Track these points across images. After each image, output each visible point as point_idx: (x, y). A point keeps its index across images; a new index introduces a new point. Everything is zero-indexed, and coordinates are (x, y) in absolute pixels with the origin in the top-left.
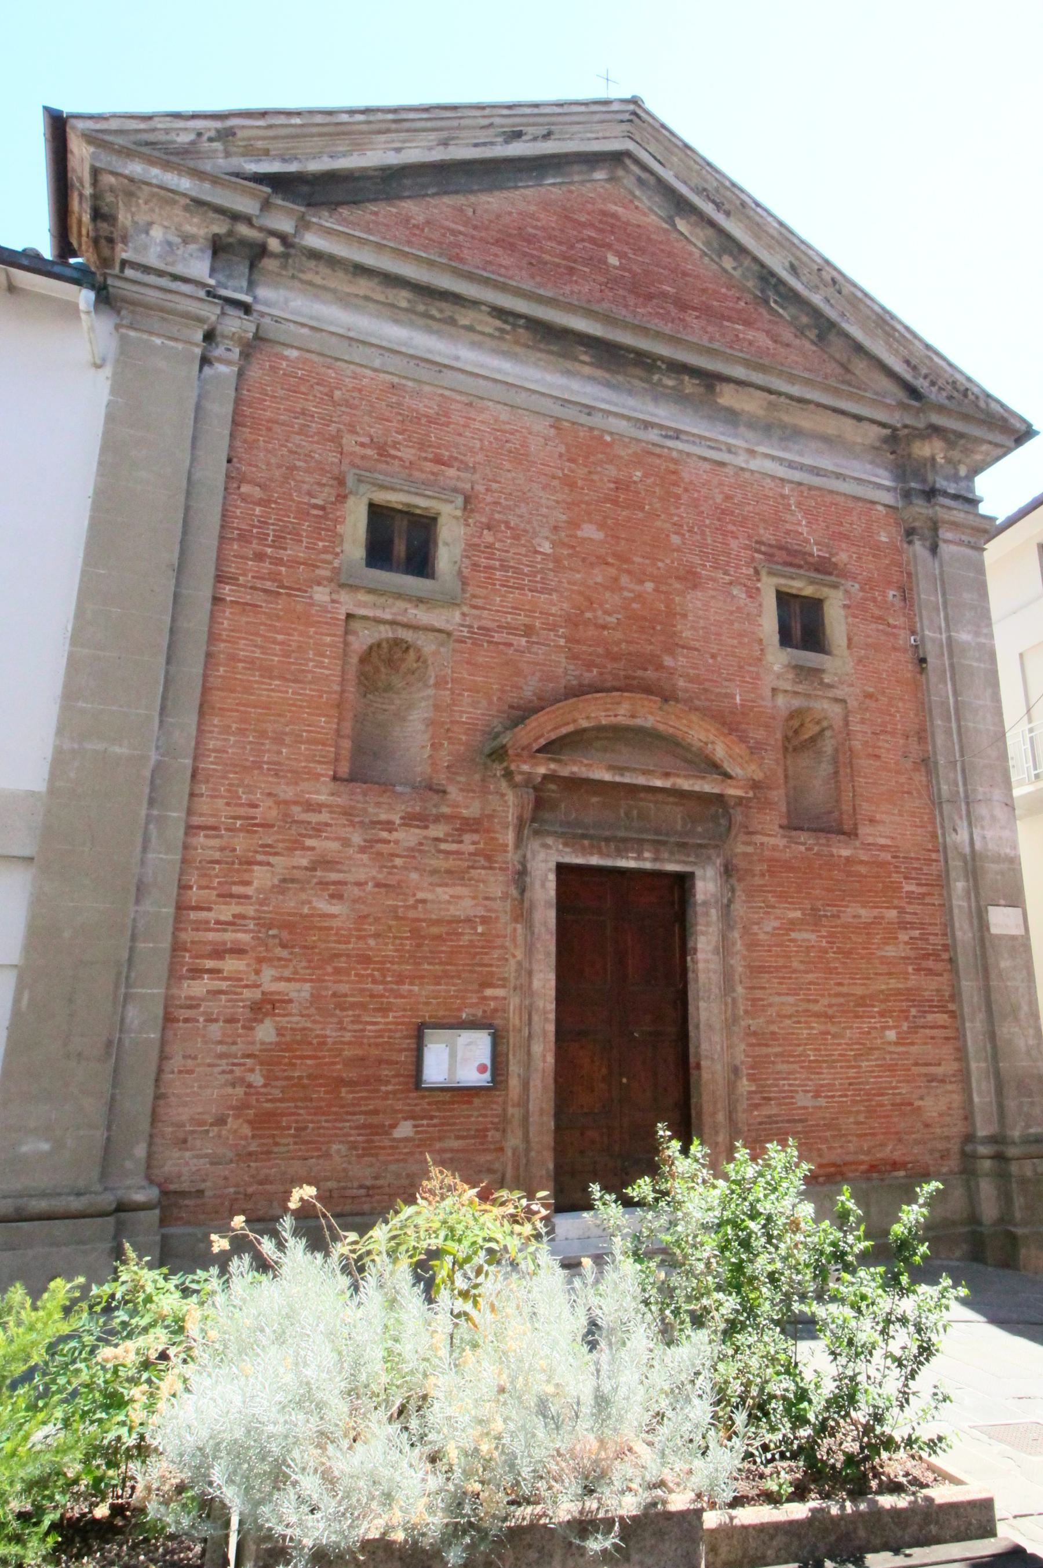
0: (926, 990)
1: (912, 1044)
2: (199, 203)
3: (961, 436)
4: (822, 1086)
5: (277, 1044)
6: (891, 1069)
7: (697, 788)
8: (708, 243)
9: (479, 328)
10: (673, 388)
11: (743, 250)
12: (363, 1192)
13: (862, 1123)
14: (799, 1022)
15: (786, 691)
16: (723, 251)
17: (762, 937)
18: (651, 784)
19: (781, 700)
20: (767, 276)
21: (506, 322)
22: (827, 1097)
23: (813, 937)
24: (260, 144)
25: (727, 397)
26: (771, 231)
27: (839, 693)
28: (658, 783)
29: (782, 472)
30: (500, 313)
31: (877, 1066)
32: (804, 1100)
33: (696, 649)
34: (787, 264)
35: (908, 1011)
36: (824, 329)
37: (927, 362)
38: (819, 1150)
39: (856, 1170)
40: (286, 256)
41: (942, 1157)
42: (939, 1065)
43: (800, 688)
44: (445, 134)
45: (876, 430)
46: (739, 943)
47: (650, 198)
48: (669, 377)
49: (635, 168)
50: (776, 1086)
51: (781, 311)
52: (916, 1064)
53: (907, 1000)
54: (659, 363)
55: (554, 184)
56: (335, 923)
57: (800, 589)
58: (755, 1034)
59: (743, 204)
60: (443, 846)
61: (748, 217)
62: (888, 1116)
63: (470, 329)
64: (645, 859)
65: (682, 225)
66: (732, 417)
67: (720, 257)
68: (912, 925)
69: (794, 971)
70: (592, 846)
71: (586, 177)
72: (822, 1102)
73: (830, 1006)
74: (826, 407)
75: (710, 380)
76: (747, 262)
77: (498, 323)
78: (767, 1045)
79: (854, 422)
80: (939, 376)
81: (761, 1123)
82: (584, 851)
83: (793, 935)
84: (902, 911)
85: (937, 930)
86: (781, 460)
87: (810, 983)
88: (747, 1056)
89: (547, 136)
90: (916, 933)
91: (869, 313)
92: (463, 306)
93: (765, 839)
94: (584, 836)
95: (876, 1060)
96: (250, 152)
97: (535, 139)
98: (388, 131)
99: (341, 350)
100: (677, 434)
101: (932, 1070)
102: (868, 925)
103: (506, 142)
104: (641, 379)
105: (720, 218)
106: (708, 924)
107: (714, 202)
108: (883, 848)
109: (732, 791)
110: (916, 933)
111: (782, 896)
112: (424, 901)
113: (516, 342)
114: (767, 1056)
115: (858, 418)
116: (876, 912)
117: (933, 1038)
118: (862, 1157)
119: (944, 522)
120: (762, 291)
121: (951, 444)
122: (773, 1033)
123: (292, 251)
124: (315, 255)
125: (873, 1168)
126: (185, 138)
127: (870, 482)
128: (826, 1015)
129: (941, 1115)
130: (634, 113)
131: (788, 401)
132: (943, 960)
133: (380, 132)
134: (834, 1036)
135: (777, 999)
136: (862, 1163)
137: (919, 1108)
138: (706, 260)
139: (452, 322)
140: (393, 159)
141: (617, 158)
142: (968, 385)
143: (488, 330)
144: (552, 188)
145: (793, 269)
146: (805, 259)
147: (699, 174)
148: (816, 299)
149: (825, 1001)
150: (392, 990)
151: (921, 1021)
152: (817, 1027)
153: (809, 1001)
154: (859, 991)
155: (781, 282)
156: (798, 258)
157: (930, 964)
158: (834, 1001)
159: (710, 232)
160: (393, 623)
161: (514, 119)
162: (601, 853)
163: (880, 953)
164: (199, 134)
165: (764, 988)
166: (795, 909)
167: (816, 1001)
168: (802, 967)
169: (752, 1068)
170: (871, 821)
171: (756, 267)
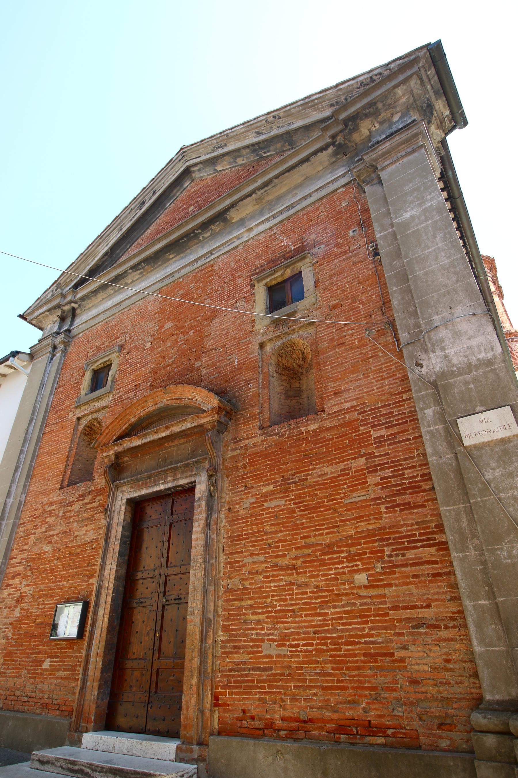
0: (402, 526)
1: (390, 585)
2: (49, 310)
3: (372, 104)
4: (286, 635)
5: (19, 617)
6: (363, 615)
7: (184, 428)
8: (230, 163)
9: (135, 279)
10: (211, 235)
11: (238, 150)
12: (26, 699)
13: (330, 675)
14: (268, 577)
15: (271, 340)
16: (235, 158)
18: (159, 437)
19: (269, 348)
20: (254, 148)
21: (140, 269)
22: (291, 646)
24: (68, 280)
25: (235, 215)
26: (241, 131)
28: (163, 435)
29: (267, 225)
30: (134, 268)
31: (345, 612)
32: (269, 649)
33: (213, 349)
34: (255, 135)
35: (383, 551)
36: (288, 138)
37: (340, 93)
38: (282, 700)
39: (322, 728)
40: (79, 306)
41: (440, 726)
42: (429, 606)
43: (278, 333)
45: (324, 156)
46: (224, 521)
47: (205, 172)
48: (206, 233)
49: (195, 169)
50: (245, 635)
51: (269, 154)
52: (396, 608)
53: (381, 540)
56: (47, 555)
57: (282, 275)
58: (232, 590)
59: (227, 135)
60: (89, 506)
61: (231, 138)
62: (359, 668)
63: (133, 281)
64: (169, 482)
65: (219, 168)
66: (242, 222)
67: (236, 162)
68: (382, 466)
69: (267, 533)
70: (143, 484)
72: (286, 651)
73: (296, 558)
74: (283, 173)
75: (221, 217)
76: (244, 152)
77: (139, 271)
79: (306, 164)
80: (352, 91)
81: (231, 670)
82: (140, 488)
83: (266, 505)
84: (370, 456)
85: (414, 462)
86: (268, 220)
88: (224, 610)
90: (388, 472)
91: (297, 109)
92: (125, 277)
93: (247, 442)
94: (138, 480)
96: (67, 284)
97: (151, 198)
98: (100, 244)
99: (92, 323)
100: (211, 252)
101: (422, 613)
102: (334, 479)
103: (141, 209)
105: (225, 150)
106: (200, 513)
107: (219, 147)
108: (348, 411)
109: (204, 420)
110: (388, 472)
111: (258, 478)
112: (76, 536)
113: (148, 273)
114: (239, 609)
115: (306, 160)
116: (342, 466)
117: (415, 576)
118: (328, 714)
119: (376, 160)
120: (257, 155)
121: (376, 114)
122: (246, 589)
123: (79, 303)
124: (83, 299)
126: (50, 295)
127: (328, 183)
128: (293, 567)
129: (435, 669)
130: (183, 152)
131: (262, 191)
132: (424, 491)
133: (98, 246)
134: (299, 586)
135: (250, 560)
136: (330, 721)
137: (402, 660)
138: (233, 169)
140: (106, 249)
141: (187, 172)
142: (370, 75)
143: (138, 277)
144: (170, 206)
145: (258, 133)
146: (258, 124)
147: (209, 145)
148: (275, 132)
149: (294, 553)
150: (57, 585)
151: (398, 560)
152: (284, 578)
153: (277, 557)
154: (327, 540)
155: (258, 143)
156: (256, 128)
157: (407, 498)
158: (300, 552)
159: (227, 158)
160: (92, 413)
161: (138, 201)
162: (148, 487)
163: (346, 501)
165: (241, 552)
166: (269, 484)
167: (284, 556)
168: (272, 529)
169: (228, 619)
170: (335, 394)
171: (248, 150)
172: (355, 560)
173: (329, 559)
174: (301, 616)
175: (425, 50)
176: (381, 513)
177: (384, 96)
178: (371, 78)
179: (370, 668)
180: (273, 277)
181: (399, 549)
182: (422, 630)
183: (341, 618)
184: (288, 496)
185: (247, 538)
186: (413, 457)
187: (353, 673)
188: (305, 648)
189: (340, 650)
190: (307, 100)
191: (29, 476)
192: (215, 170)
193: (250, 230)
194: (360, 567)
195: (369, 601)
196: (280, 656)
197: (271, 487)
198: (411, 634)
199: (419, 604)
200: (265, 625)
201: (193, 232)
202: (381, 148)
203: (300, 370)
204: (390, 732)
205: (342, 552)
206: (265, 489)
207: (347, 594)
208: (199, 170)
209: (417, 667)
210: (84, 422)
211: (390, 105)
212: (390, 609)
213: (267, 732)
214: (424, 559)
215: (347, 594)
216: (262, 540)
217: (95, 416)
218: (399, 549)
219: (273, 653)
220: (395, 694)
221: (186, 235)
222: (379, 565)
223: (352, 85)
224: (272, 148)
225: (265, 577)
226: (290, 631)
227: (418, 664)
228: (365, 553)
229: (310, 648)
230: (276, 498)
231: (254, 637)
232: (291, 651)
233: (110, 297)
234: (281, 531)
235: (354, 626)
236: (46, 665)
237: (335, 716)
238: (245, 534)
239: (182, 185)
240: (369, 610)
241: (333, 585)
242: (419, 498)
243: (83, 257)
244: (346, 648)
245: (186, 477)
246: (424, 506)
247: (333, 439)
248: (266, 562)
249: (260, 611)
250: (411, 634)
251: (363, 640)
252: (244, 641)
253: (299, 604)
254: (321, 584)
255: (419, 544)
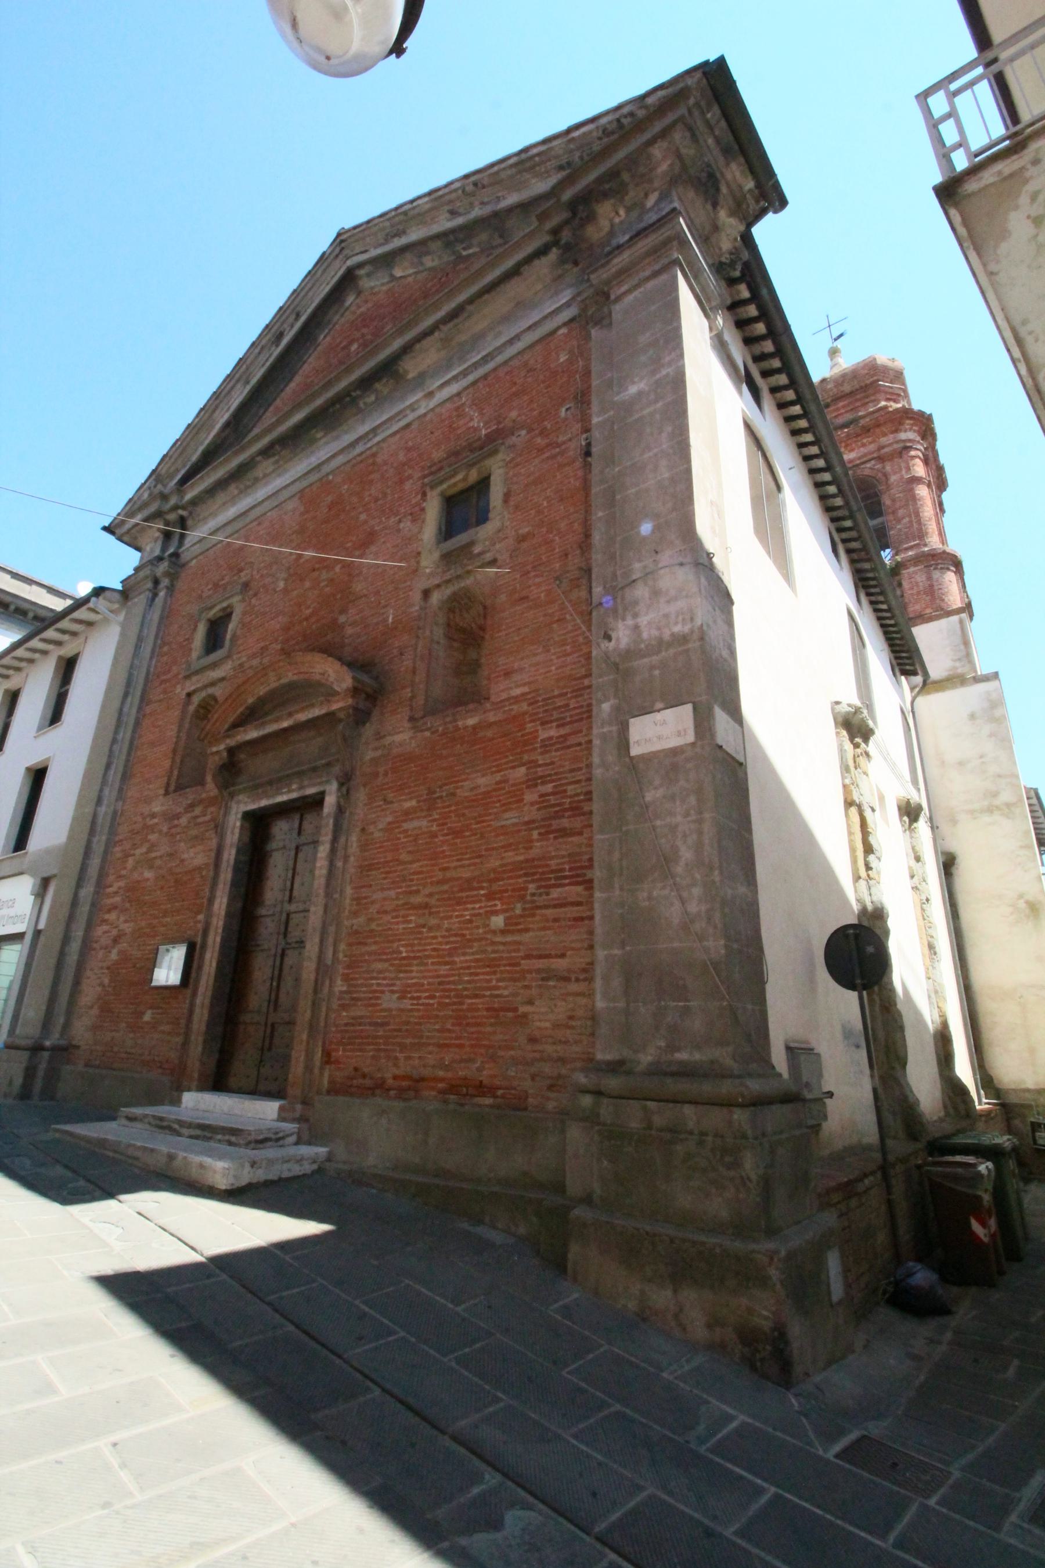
0: (552, 858)
1: (527, 930)
3: (613, 174)
4: (409, 986)
10: (377, 399)
13: (449, 1031)
14: (397, 917)
15: (438, 586)
17: (377, 834)
19: (436, 598)
20: (448, 238)
23: (424, 823)
24: (173, 469)
25: (411, 367)
27: (488, 557)
28: (285, 724)
30: (266, 452)
32: (389, 1001)
35: (526, 889)
37: (572, 146)
38: (396, 1058)
40: (191, 513)
41: (551, 1087)
42: (563, 956)
43: (447, 577)
44: (244, 377)
45: (543, 266)
49: (362, 272)
50: (366, 986)
51: (471, 251)
52: (528, 957)
53: (526, 875)
54: (354, 394)
55: (325, 337)
57: (465, 479)
58: (357, 932)
59: (405, 213)
62: (478, 1025)
63: (265, 476)
64: (293, 791)
65: (398, 272)
67: (422, 264)
68: (544, 780)
69: (405, 863)
71: (342, 311)
72: (407, 1004)
73: (431, 895)
74: (480, 294)
77: (272, 460)
78: (366, 944)
81: (346, 1024)
83: (405, 826)
85: (580, 776)
86: (455, 378)
87: (414, 873)
88: (346, 956)
89: (298, 316)
90: (549, 788)
91: (509, 172)
95: (476, 953)
96: (171, 477)
97: (292, 326)
98: (217, 407)
100: (374, 431)
103: (277, 346)
104: (356, 415)
105: (403, 241)
106: (326, 835)
108: (517, 700)
110: (549, 788)
117: (556, 920)
118: (441, 1073)
119: (608, 282)
122: (372, 931)
124: (194, 502)
125: (453, 1088)
126: (146, 495)
128: (426, 906)
129: (556, 1026)
130: (343, 241)
131: (451, 325)
136: (442, 1080)
137: (525, 1015)
139: (257, 480)
140: (226, 416)
141: (349, 279)
142: (617, 115)
143: (271, 469)
144: (324, 339)
145: (453, 213)
148: (477, 212)
151: (541, 900)
154: (466, 874)
155: (453, 231)
157: (565, 823)
159: (408, 255)
160: (205, 687)
161: (272, 332)
162: (268, 797)
164: (149, 488)
165: (371, 886)
166: (411, 799)
167: (418, 892)
169: (348, 967)
171: (439, 243)
172: (494, 899)
173: (467, 897)
174: (426, 964)
175: (698, 75)
176: (531, 841)
177: (632, 161)
178: (618, 120)
179: (491, 1025)
180: (453, 481)
181: (545, 887)
182: (551, 983)
183: (469, 968)
184: (430, 816)
185: (379, 868)
186: (580, 769)
187: (473, 1029)
188: (427, 1001)
189: (462, 1003)
190: (523, 156)
191: (126, 777)
192: (392, 276)
193: (430, 395)
194: (499, 907)
195: (501, 948)
196: (402, 1010)
197: (414, 803)
198: (540, 986)
199: (553, 953)
200: (387, 974)
201: (349, 395)
202: (616, 261)
203: (481, 633)
204: (500, 1092)
205: (482, 888)
206: (407, 805)
207: (480, 940)
208: (368, 275)
209: (538, 1024)
210: (196, 700)
211: (643, 175)
212: (523, 958)
213: (378, 1092)
214: (570, 900)
215: (480, 940)
216: (395, 871)
217: (210, 691)
218: (545, 887)
219: (393, 1005)
220: (512, 1053)
221: (338, 399)
222: (519, 905)
223: (590, 132)
224: (475, 241)
225: (393, 918)
226: (414, 981)
227: (540, 1021)
228: (506, 891)
229: (431, 1001)
230: (418, 818)
231: (375, 988)
232: (412, 1004)
233: (233, 500)
234: (418, 861)
235: (481, 977)
236: (147, 1017)
237: (449, 1075)
238: (377, 863)
239: (344, 301)
240: (502, 958)
241: (467, 929)
242: (577, 823)
243: (193, 430)
244: (470, 1001)
245: (314, 785)
246: (580, 833)
247: (493, 739)
248: (397, 899)
249: (385, 957)
250: (540, 986)
251: (488, 993)
252: (364, 992)
253: (425, 950)
254: (454, 927)
255: (567, 881)
